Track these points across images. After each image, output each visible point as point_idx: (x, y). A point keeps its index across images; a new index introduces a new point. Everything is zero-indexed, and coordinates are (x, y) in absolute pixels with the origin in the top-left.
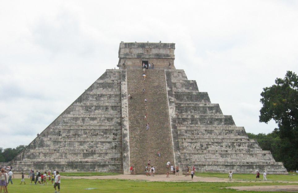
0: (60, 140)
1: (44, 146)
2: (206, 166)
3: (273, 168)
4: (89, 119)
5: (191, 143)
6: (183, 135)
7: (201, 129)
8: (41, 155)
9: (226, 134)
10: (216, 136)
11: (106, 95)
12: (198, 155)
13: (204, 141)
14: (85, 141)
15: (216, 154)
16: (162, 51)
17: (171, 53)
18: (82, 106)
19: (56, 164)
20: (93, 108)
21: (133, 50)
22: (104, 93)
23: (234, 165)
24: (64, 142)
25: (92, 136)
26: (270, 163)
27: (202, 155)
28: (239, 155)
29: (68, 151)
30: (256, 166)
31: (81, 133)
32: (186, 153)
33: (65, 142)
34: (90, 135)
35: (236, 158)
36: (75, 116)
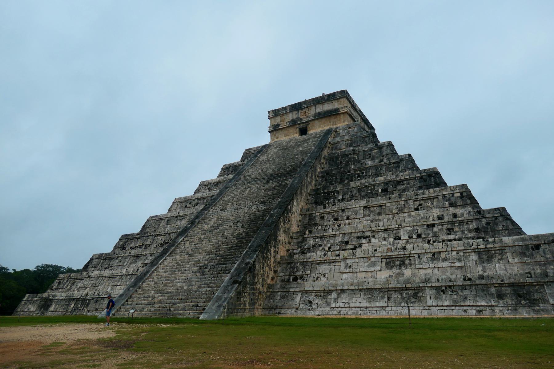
2: (334, 295)
6: (316, 225)
7: (354, 206)
9: (417, 209)
10: (391, 216)
15: (373, 259)
16: (327, 107)
27: (336, 264)
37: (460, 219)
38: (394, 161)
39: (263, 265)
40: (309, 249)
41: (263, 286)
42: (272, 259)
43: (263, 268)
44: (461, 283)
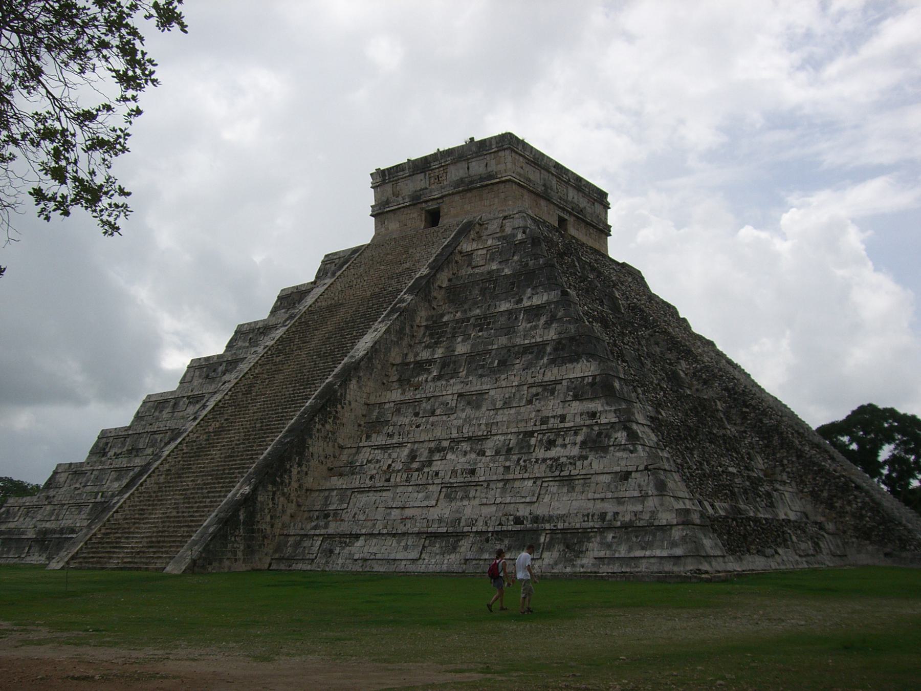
2: (360, 542)
3: (628, 539)
5: (384, 448)
6: (387, 422)
7: (444, 393)
9: (530, 402)
10: (492, 412)
12: (371, 494)
13: (427, 439)
15: (431, 488)
16: (477, 168)
17: (501, 167)
21: (401, 184)
23: (464, 535)
26: (620, 517)
27: (384, 494)
28: (517, 484)
30: (553, 531)
32: (333, 490)
35: (498, 501)
37: (567, 425)
38: (539, 303)
39: (274, 493)
40: (362, 466)
41: (272, 526)
42: (295, 485)
43: (273, 499)
44: (510, 528)
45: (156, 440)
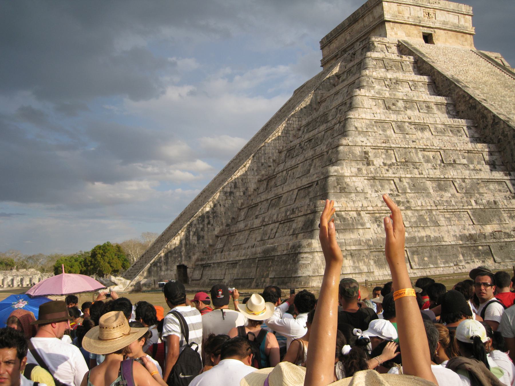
0: (387, 175)
1: (350, 193)
4: (413, 127)
8: (366, 217)
11: (407, 82)
14: (446, 177)
18: (373, 98)
19: (434, 244)
20: (401, 104)
22: (400, 75)
24: (397, 181)
25: (444, 166)
29: (433, 204)
31: (419, 159)
33: (400, 181)
34: (440, 165)
36: (378, 117)
45: (428, 157)
